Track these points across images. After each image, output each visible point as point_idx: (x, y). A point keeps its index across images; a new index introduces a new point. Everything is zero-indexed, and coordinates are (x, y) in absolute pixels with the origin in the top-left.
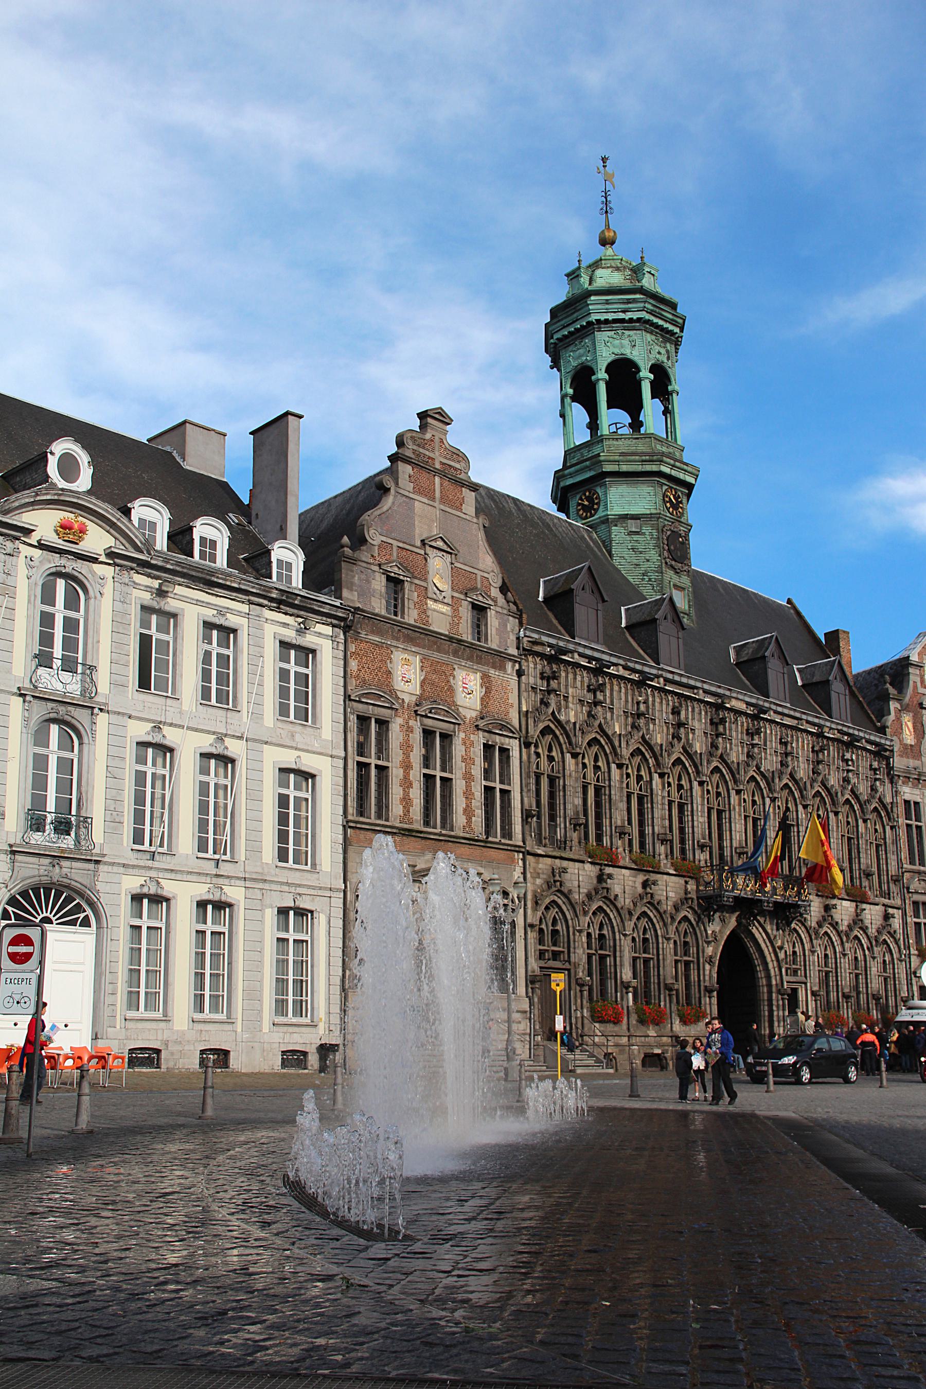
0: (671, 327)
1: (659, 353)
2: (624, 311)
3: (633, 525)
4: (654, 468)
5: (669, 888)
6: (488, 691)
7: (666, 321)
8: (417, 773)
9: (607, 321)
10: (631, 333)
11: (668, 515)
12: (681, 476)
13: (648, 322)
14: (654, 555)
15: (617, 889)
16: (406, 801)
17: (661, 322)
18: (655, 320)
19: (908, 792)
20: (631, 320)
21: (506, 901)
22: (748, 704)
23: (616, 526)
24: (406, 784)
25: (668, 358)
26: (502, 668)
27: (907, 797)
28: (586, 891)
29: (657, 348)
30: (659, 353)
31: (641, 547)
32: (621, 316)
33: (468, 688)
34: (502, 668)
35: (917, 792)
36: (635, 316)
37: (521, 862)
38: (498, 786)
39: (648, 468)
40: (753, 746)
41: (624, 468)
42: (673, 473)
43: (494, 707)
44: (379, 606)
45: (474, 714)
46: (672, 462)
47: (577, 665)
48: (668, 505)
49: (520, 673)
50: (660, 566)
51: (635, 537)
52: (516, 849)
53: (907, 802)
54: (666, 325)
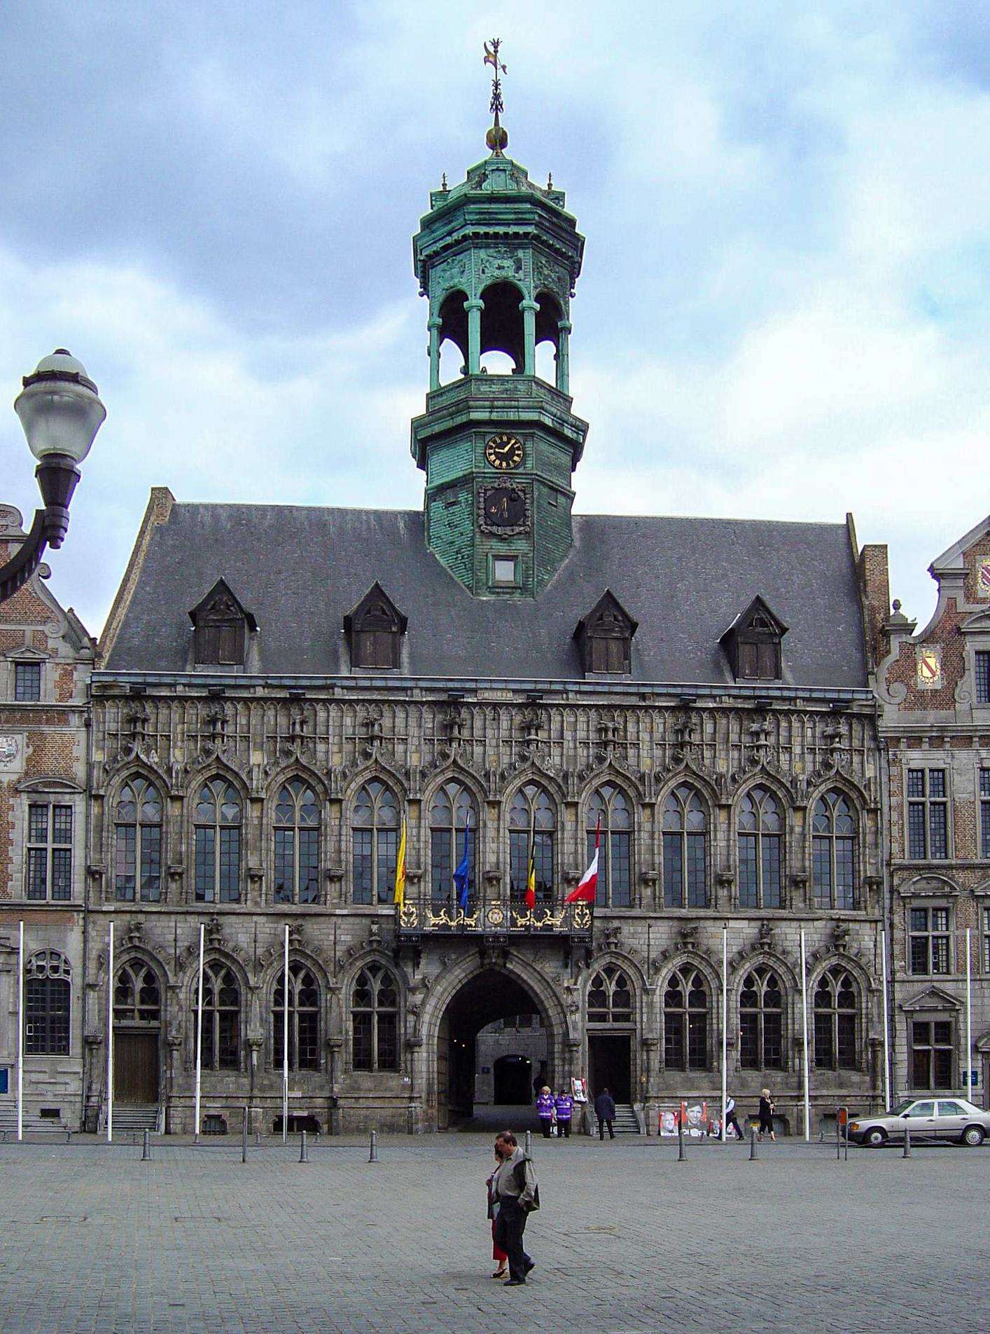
0: (521, 230)
1: (500, 268)
2: (450, 234)
4: (463, 419)
5: (337, 933)
6: (38, 750)
7: (509, 225)
9: (436, 254)
12: (512, 416)
13: (476, 235)
14: (467, 526)
15: (243, 940)
17: (501, 230)
18: (491, 230)
19: (916, 758)
20: (457, 242)
21: (55, 963)
22: (515, 691)
25: (518, 268)
26: (67, 723)
27: (913, 765)
28: (186, 944)
30: (500, 268)
31: (456, 520)
32: (449, 240)
34: (67, 723)
35: (940, 754)
36: (456, 236)
37: (81, 922)
38: (50, 846)
40: (529, 742)
42: (495, 416)
43: (50, 764)
45: (14, 777)
46: (487, 403)
47: (183, 699)
48: (493, 457)
49: (88, 725)
50: (473, 538)
51: (451, 510)
52: (76, 908)
54: (512, 230)
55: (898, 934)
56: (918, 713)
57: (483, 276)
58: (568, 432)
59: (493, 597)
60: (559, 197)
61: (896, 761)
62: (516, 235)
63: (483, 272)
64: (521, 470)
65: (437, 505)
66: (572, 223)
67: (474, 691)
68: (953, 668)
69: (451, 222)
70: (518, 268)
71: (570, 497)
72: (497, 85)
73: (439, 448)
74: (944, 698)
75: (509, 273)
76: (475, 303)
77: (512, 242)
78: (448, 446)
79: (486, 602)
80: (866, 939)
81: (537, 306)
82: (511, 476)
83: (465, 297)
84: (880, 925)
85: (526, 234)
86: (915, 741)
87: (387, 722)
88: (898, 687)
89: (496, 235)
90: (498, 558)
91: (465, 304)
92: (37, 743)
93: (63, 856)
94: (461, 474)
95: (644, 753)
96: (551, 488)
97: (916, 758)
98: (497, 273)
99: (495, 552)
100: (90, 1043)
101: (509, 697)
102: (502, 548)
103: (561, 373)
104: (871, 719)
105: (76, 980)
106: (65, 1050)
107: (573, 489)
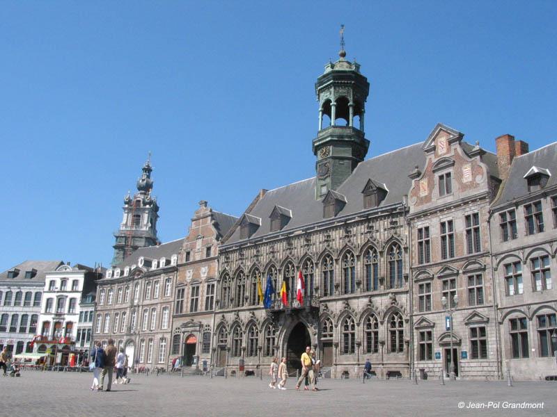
7: (325, 83)
8: (205, 296)
12: (324, 141)
16: (187, 307)
17: (326, 84)
19: (420, 224)
24: (187, 302)
27: (419, 227)
33: (204, 272)
35: (427, 221)
43: (211, 275)
44: (184, 262)
53: (420, 230)
55: (415, 296)
56: (420, 206)
61: (414, 227)
67: (293, 233)
68: (431, 186)
74: (428, 199)
80: (403, 300)
84: (408, 295)
85: (331, 83)
86: (419, 216)
87: (276, 247)
88: (415, 198)
90: (322, 186)
92: (209, 267)
93: (212, 297)
95: (337, 242)
97: (420, 224)
100: (214, 350)
101: (301, 232)
104: (405, 212)
105: (212, 333)
106: (208, 352)
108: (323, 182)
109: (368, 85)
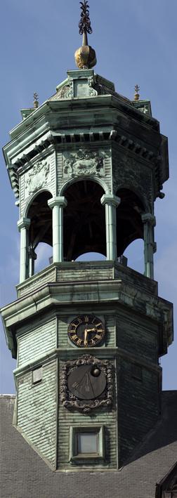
3: (37, 375)
7: (89, 127)
9: (23, 161)
10: (43, 162)
11: (76, 348)
12: (93, 299)
14: (51, 404)
20: (41, 148)
23: (22, 383)
25: (99, 167)
29: (78, 162)
31: (40, 397)
32: (32, 147)
36: (39, 142)
39: (42, 305)
41: (23, 316)
42: (76, 300)
57: (65, 176)
58: (150, 311)
59: (75, 470)
60: (148, 105)
62: (96, 136)
63: (66, 172)
64: (103, 347)
65: (25, 387)
66: (155, 125)
69: (34, 130)
70: (99, 167)
71: (157, 375)
72: (84, 7)
73: (22, 334)
75: (93, 170)
76: (55, 199)
77: (91, 145)
78: (32, 330)
79: (70, 474)
81: (118, 200)
82: (93, 353)
83: (49, 195)
89: (77, 138)
91: (50, 202)
94: (45, 355)
96: (137, 365)
98: (77, 172)
99: (77, 425)
102: (85, 421)
103: (149, 261)
107: (161, 366)
108: (85, 421)
109: (168, 177)
